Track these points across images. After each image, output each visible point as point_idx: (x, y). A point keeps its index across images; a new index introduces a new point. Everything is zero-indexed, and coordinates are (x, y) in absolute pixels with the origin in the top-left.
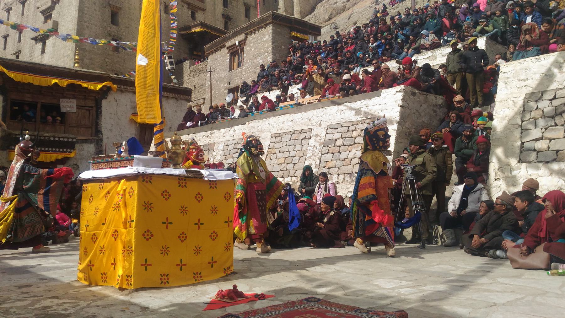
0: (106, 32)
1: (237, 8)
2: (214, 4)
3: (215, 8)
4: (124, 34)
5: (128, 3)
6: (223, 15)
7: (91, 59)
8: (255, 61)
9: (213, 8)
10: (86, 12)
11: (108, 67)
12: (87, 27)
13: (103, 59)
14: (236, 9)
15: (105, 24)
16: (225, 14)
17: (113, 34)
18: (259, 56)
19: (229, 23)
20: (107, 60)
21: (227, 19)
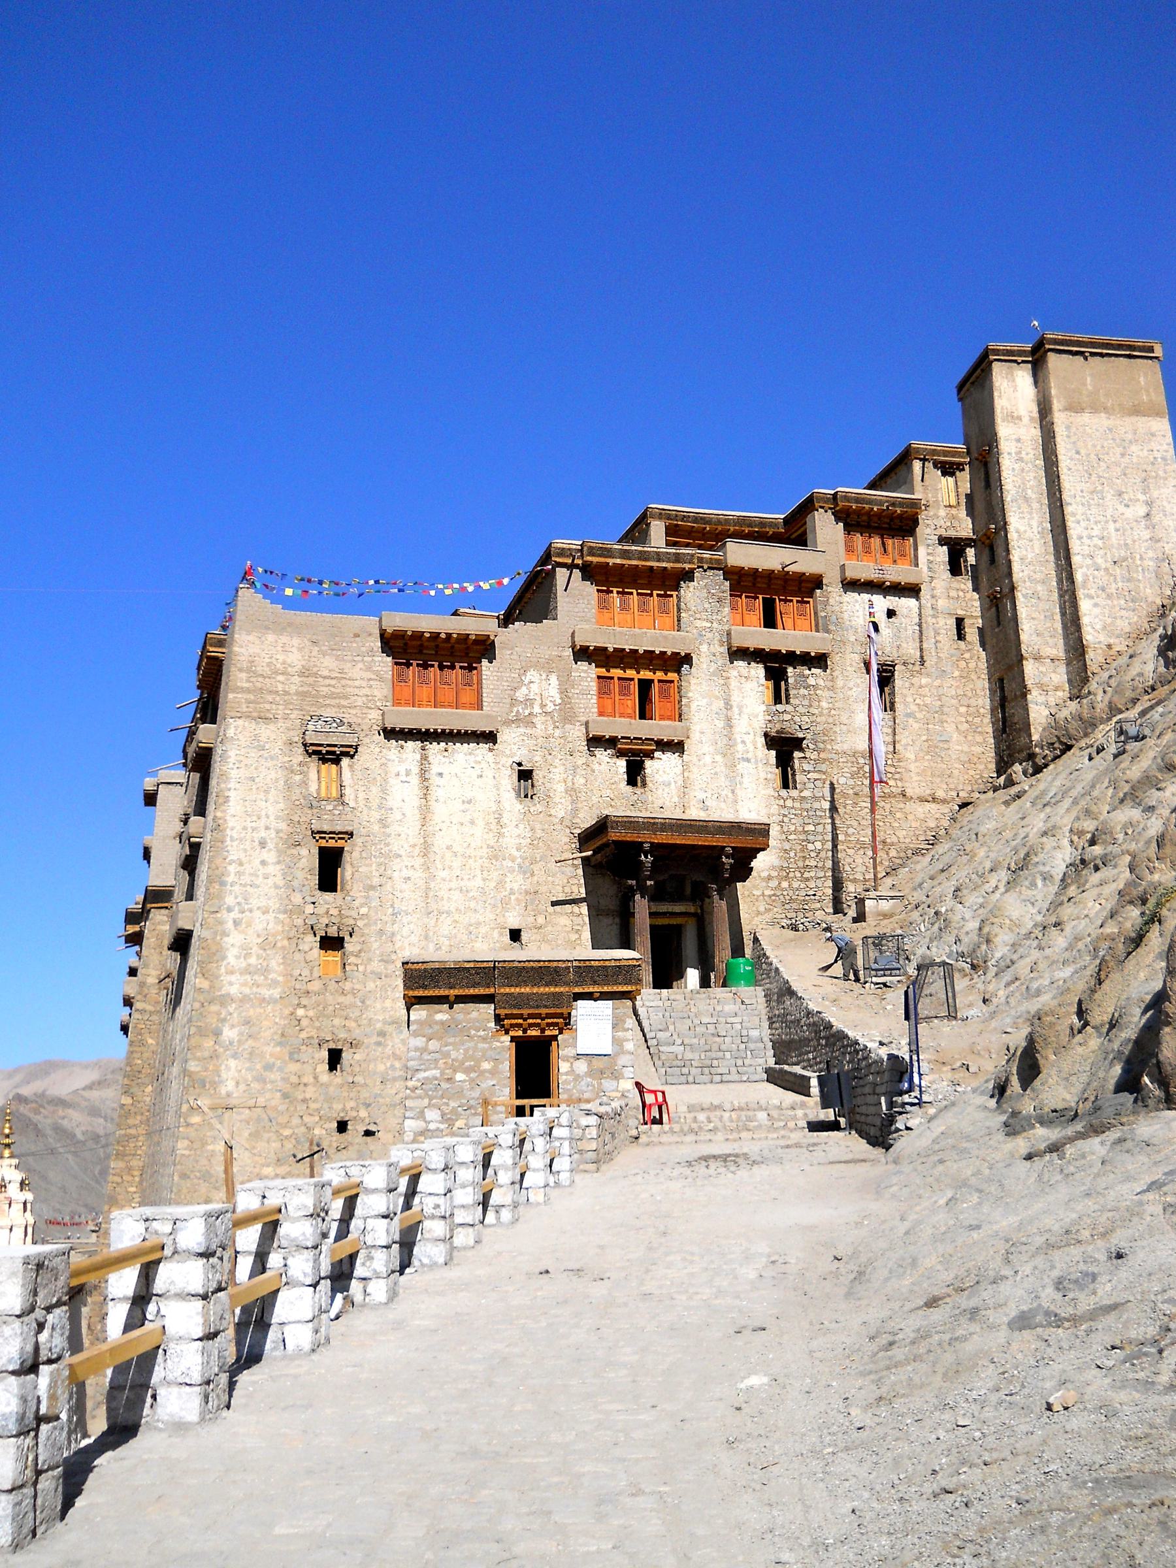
0: (299, 922)
1: (832, 689)
2: (728, 706)
3: (729, 719)
4: (364, 910)
5: (380, 807)
6: (766, 735)
7: (247, 1022)
9: (720, 724)
10: (230, 879)
11: (303, 1035)
12: (236, 923)
13: (287, 1012)
14: (827, 694)
15: (297, 899)
17: (325, 921)
19: (797, 754)
20: (300, 1012)
21: (784, 747)
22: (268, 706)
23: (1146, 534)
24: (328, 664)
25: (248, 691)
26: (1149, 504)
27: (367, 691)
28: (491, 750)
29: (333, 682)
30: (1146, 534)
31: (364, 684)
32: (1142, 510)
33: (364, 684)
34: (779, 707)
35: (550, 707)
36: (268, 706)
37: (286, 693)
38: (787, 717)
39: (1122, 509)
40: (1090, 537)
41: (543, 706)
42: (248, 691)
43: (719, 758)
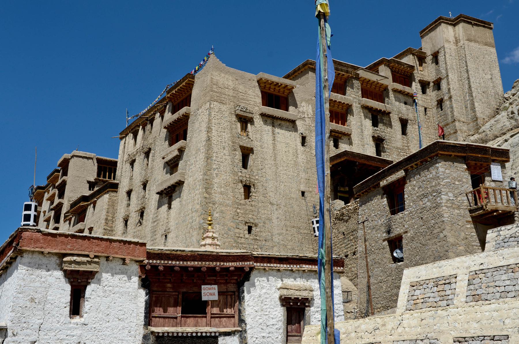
3: (362, 130)
6: (373, 137)
8: (421, 203)
16: (376, 135)
18: (425, 196)
22: (223, 99)
23: (491, 85)
24: (241, 88)
25: (216, 92)
26: (491, 75)
27: (254, 100)
28: (293, 127)
29: (243, 94)
30: (491, 85)
31: (253, 97)
32: (490, 77)
33: (253, 97)
34: (375, 128)
35: (310, 116)
36: (223, 99)
37: (229, 95)
38: (378, 132)
39: (484, 75)
40: (476, 83)
41: (308, 115)
42: (216, 92)
43: (360, 142)
